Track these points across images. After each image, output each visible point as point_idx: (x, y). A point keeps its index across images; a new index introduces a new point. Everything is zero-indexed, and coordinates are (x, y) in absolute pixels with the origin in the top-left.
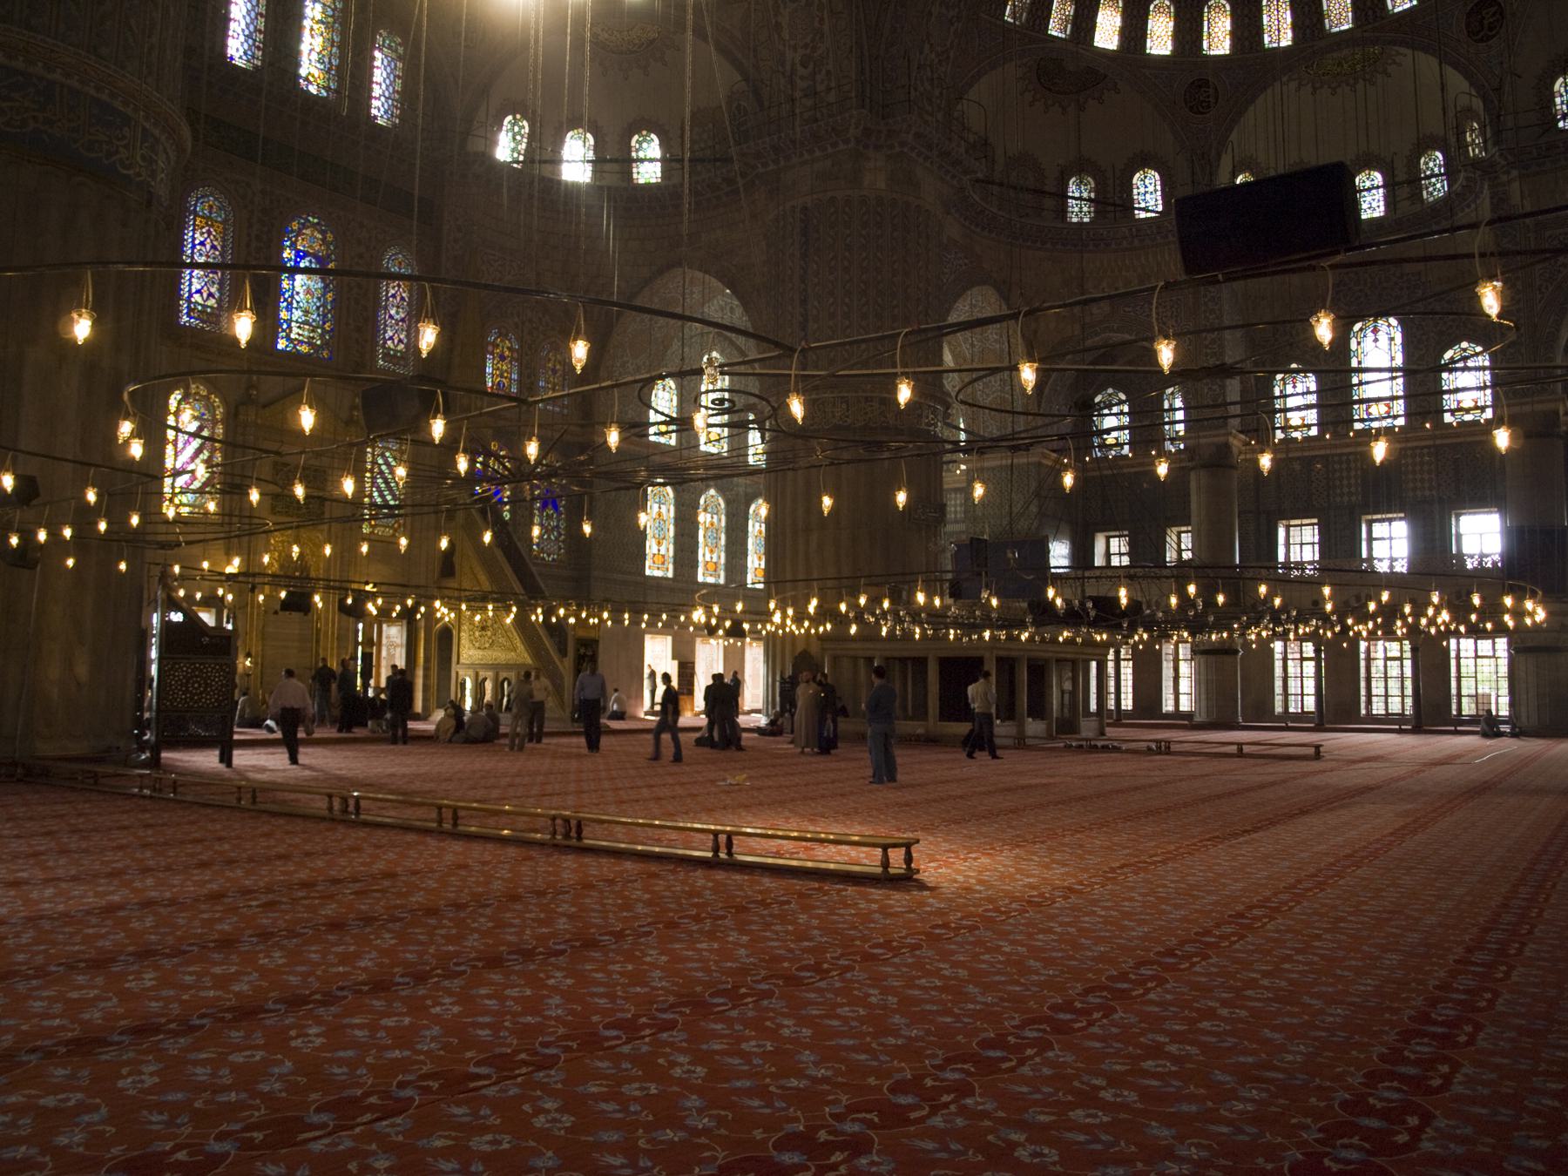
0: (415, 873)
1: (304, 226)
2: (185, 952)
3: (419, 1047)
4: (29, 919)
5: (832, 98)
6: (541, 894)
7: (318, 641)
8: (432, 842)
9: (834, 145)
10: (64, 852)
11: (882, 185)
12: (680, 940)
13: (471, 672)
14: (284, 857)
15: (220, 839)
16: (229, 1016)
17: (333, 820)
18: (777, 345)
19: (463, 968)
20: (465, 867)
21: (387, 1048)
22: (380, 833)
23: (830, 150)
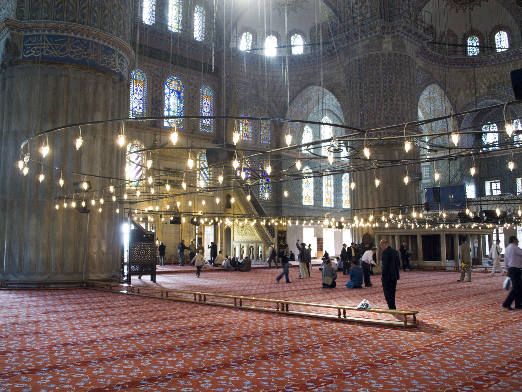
0: (230, 324)
1: (172, 80)
2: (158, 353)
3: (244, 387)
4: (103, 340)
5: (369, 15)
6: (277, 332)
7: (182, 234)
8: (233, 312)
9: (371, 34)
10: (107, 315)
11: (391, 48)
12: (330, 350)
13: (238, 244)
14: (182, 317)
15: (159, 310)
16: (178, 375)
17: (196, 303)
18: (359, 130)
19: (254, 360)
20: (247, 321)
21: (233, 388)
22: (214, 308)
23: (369, 36)
